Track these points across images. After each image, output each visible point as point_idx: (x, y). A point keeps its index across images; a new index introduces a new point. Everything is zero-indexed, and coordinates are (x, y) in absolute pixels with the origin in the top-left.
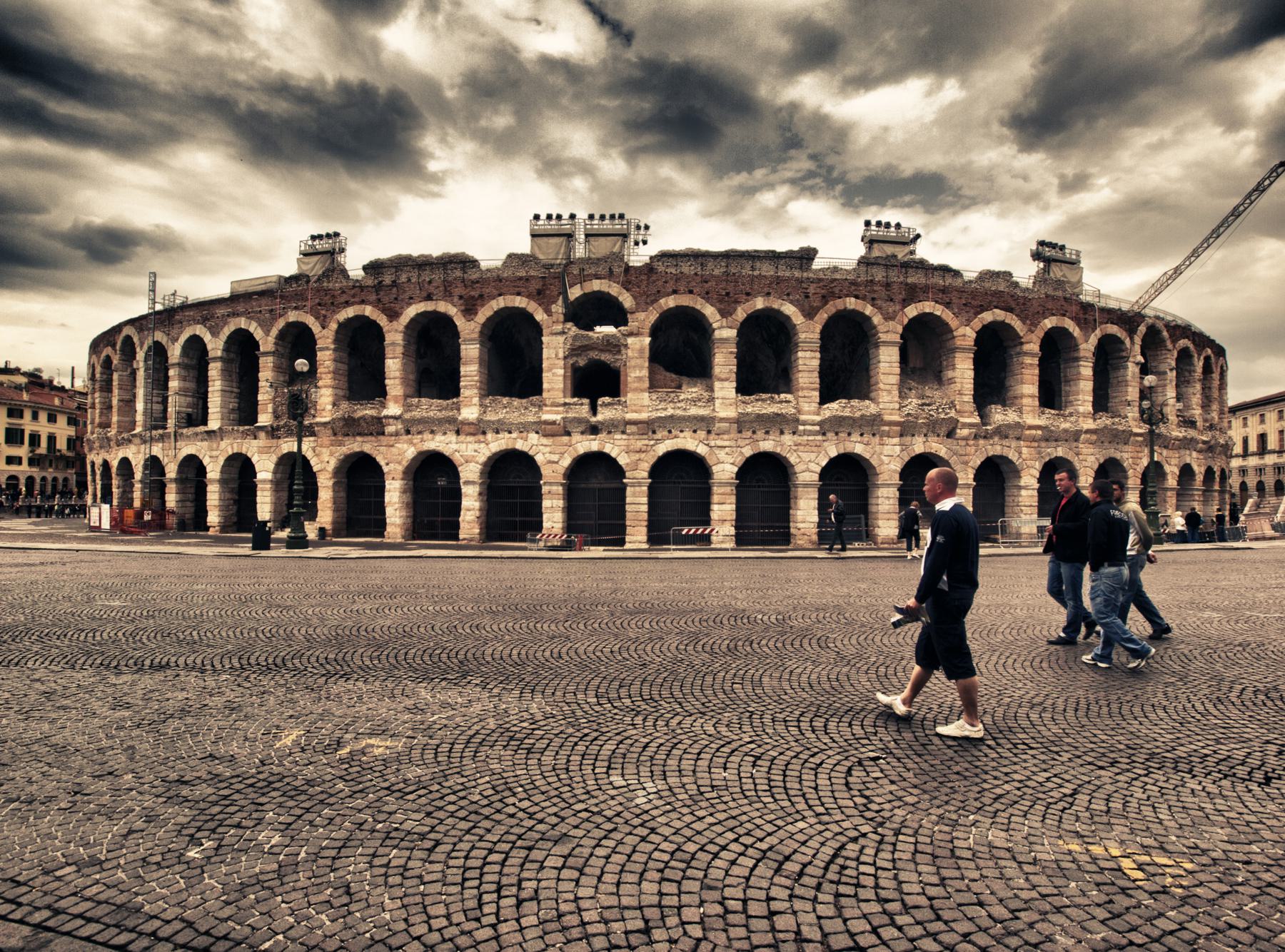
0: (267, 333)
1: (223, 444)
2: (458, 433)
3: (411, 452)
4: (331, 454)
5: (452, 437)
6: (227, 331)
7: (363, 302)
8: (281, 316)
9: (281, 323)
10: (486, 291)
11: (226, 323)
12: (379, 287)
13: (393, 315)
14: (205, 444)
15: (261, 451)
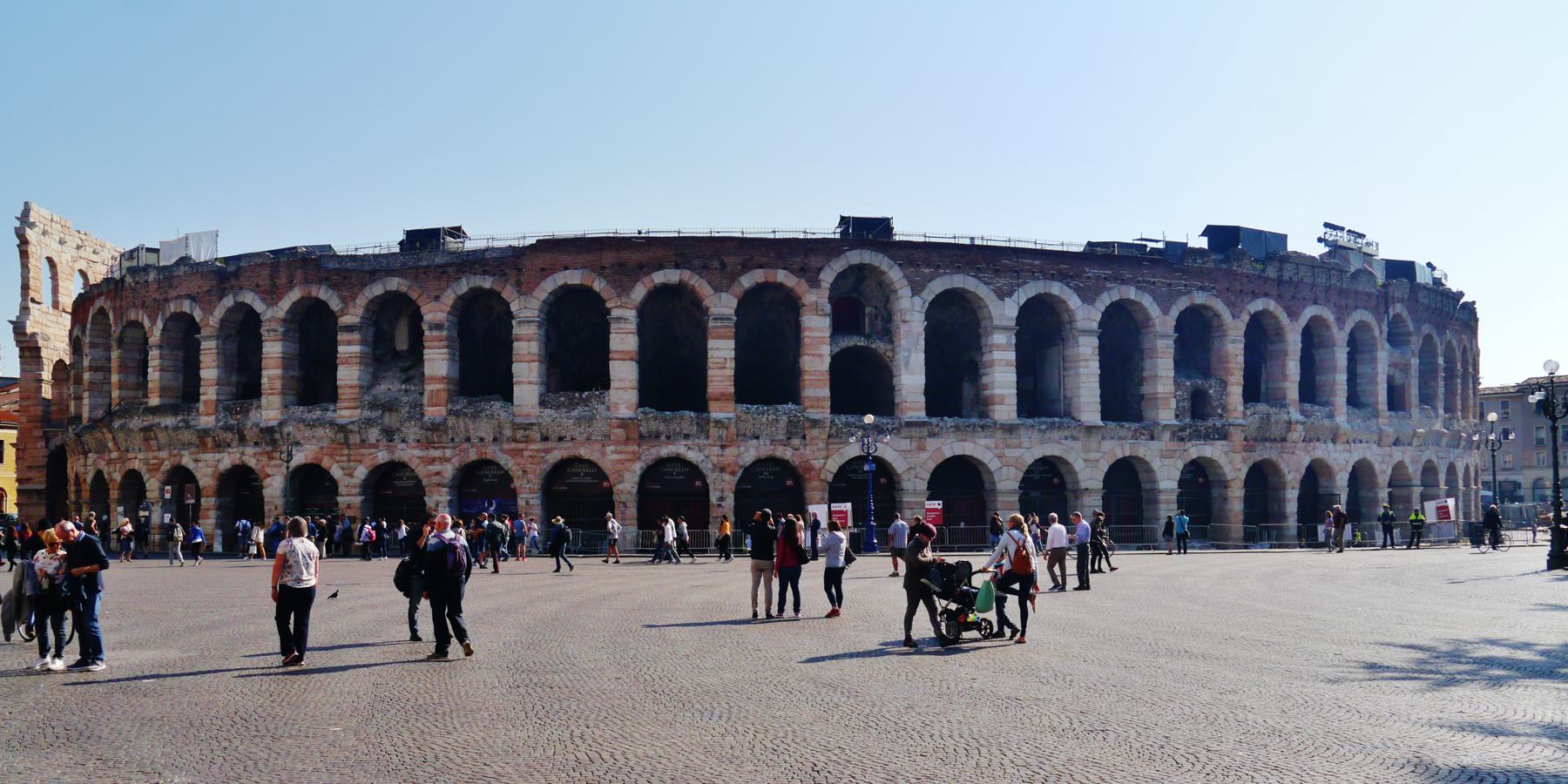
0: (1166, 311)
1: (1107, 445)
2: (1334, 441)
3: (1306, 461)
4: (1244, 461)
5: (1330, 445)
6: (1105, 300)
7: (1266, 295)
8: (1181, 293)
9: (1183, 303)
10: (1350, 302)
11: (1105, 289)
12: (1280, 281)
13: (1293, 315)
14: (1078, 445)
15: (1164, 455)
